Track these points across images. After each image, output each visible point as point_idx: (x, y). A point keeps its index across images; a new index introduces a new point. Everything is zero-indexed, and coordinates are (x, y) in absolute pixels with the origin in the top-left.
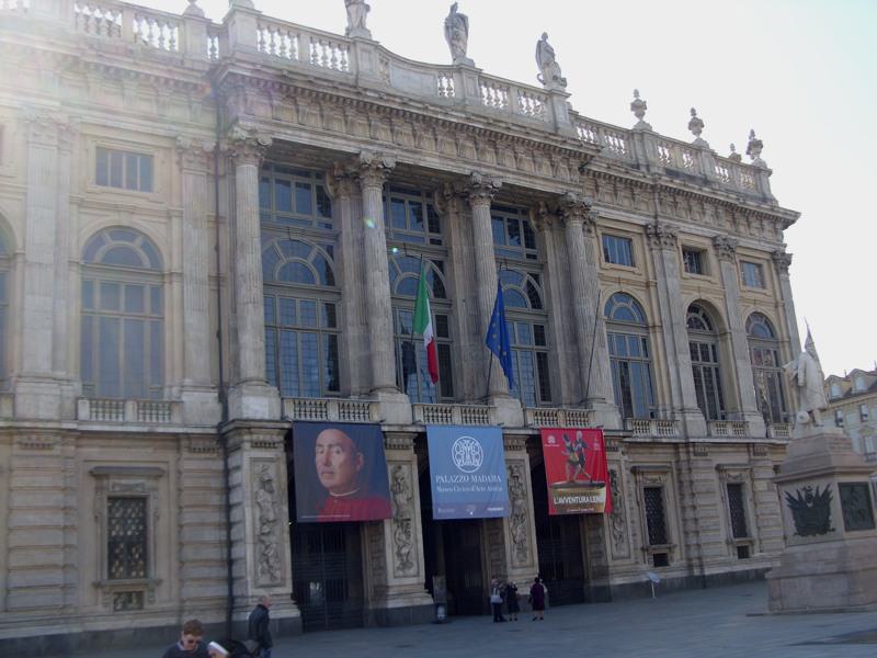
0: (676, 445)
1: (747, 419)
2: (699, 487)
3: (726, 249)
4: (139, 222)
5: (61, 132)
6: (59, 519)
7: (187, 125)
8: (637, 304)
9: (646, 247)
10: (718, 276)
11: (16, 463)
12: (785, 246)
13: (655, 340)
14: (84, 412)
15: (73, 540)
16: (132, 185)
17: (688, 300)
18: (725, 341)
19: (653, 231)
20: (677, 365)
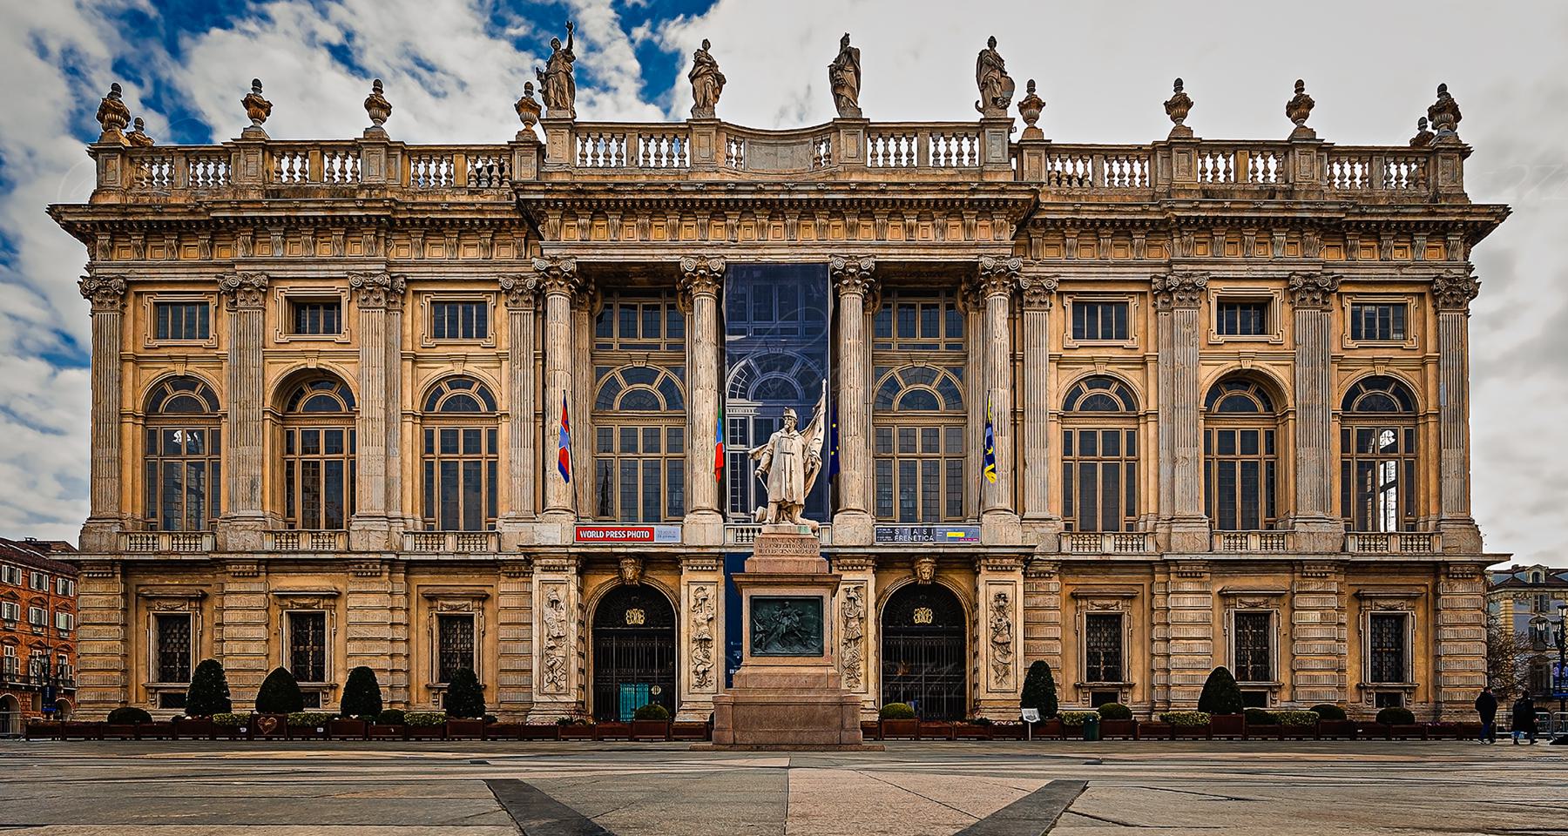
0: (1150, 565)
1: (1299, 527)
2: (1173, 616)
3: (1312, 291)
4: (471, 368)
5: (387, 294)
6: (387, 632)
7: (511, 264)
8: (1126, 392)
9: (1151, 310)
10: (1287, 331)
11: (352, 588)
12: (1470, 268)
13: (1148, 433)
14: (409, 544)
15: (401, 648)
16: (467, 335)
17: (1208, 375)
18: (1285, 423)
19: (1157, 284)
20: (1174, 461)
